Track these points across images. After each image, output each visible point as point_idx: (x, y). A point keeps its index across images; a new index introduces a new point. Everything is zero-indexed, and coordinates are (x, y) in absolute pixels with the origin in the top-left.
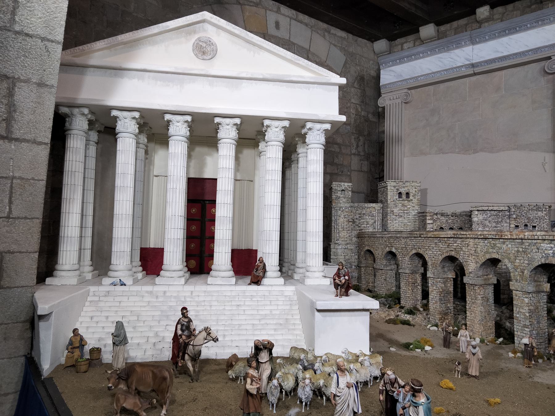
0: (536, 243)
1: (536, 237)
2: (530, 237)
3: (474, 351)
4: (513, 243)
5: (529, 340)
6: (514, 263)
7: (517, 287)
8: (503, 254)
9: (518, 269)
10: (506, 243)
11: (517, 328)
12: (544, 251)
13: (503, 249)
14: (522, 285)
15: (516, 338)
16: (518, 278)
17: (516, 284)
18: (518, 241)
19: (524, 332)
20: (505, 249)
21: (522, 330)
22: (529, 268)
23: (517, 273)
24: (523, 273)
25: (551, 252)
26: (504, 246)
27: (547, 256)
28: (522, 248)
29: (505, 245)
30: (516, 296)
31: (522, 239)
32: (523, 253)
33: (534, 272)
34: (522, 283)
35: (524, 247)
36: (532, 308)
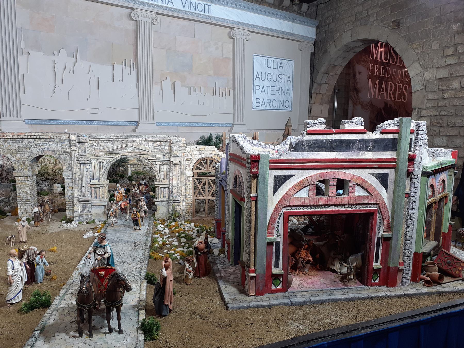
0: (34, 141)
1: (35, 137)
2: (29, 137)
3: (24, 224)
4: (15, 142)
5: (38, 209)
6: (16, 156)
7: (20, 174)
8: (5, 150)
9: (19, 160)
10: (7, 142)
11: (20, 203)
12: (41, 147)
13: (4, 146)
14: (24, 172)
15: (19, 211)
16: (20, 167)
17: (19, 172)
18: (18, 139)
19: (26, 205)
20: (6, 146)
21: (24, 204)
22: (29, 159)
23: (19, 164)
24: (24, 163)
25: (46, 147)
26: (6, 144)
27: (43, 150)
28: (23, 145)
29: (7, 143)
30: (19, 180)
31: (23, 138)
32: (23, 149)
33: (32, 162)
34: (23, 170)
35: (24, 144)
36: (31, 187)
